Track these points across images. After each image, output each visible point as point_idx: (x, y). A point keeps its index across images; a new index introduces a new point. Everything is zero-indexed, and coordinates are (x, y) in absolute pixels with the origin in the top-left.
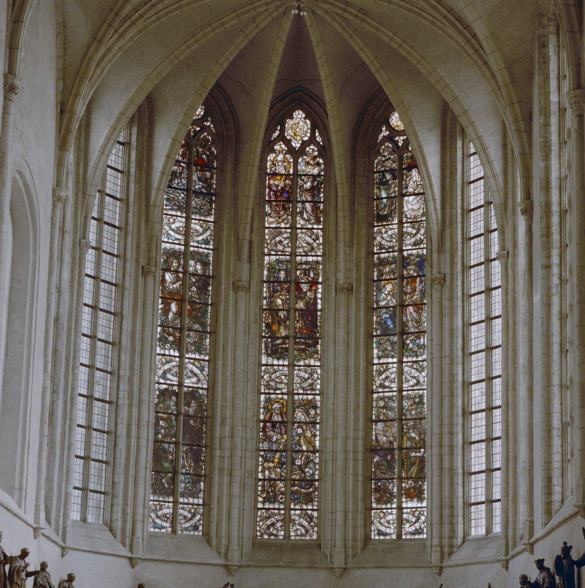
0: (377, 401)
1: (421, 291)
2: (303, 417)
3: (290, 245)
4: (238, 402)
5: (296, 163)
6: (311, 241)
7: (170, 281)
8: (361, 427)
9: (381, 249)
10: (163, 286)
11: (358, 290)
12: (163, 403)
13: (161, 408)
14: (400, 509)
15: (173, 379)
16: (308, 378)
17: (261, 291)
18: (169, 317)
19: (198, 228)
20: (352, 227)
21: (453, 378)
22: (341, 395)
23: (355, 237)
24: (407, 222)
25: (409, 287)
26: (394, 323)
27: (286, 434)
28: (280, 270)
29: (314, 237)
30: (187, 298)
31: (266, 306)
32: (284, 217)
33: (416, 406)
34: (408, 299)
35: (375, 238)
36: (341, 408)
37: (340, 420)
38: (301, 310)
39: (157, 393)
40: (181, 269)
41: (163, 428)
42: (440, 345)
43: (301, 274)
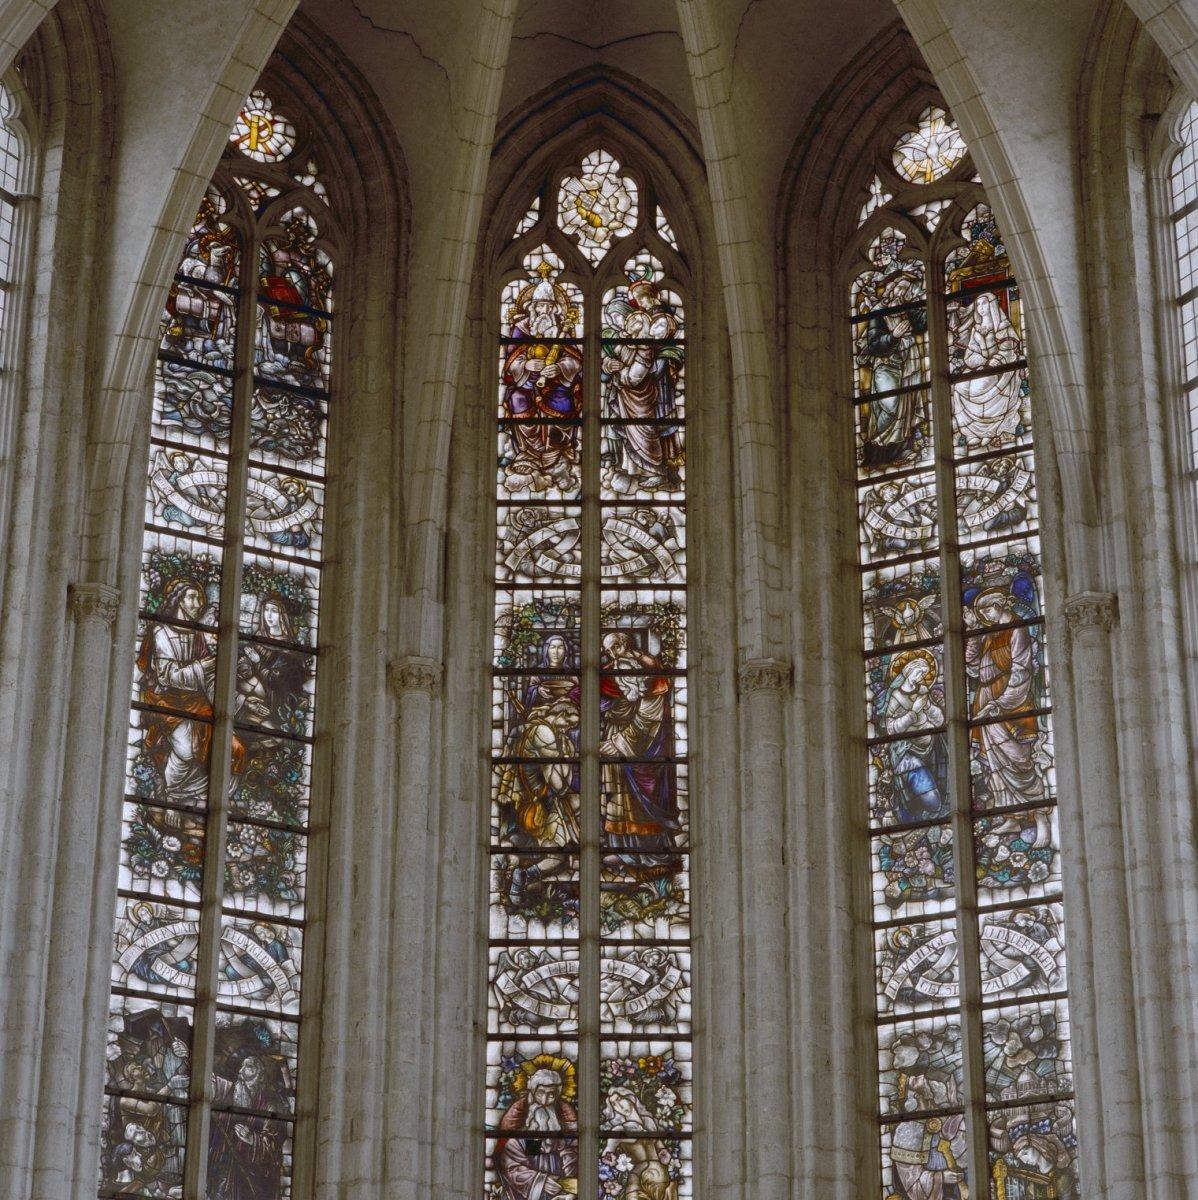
0: (891, 1049)
1: (1029, 670)
2: (634, 1116)
3: (578, 554)
4: (403, 1056)
5: (594, 307)
6: (647, 541)
7: (170, 655)
8: (840, 1136)
9: (883, 550)
10: (147, 669)
11: (813, 681)
12: (138, 1060)
13: (131, 1079)
15: (177, 981)
16: (650, 984)
17: (485, 702)
18: (168, 771)
19: (271, 492)
20: (784, 482)
21: (1167, 936)
22: (766, 1030)
23: (796, 513)
24: (967, 460)
25: (985, 662)
26: (939, 784)
27: (575, 1175)
28: (545, 635)
29: (657, 528)
30: (231, 711)
31: (501, 748)
32: (557, 471)
33: (1031, 1057)
34: (983, 701)
35: (861, 522)
36: (769, 1071)
37: (766, 1112)
38: (621, 759)
39: (120, 1025)
40: (209, 620)
41: (140, 1148)
42: (1112, 825)
43: (616, 645)
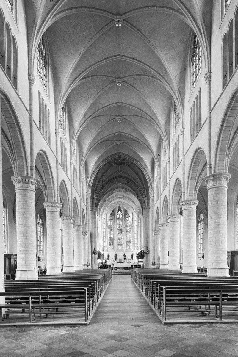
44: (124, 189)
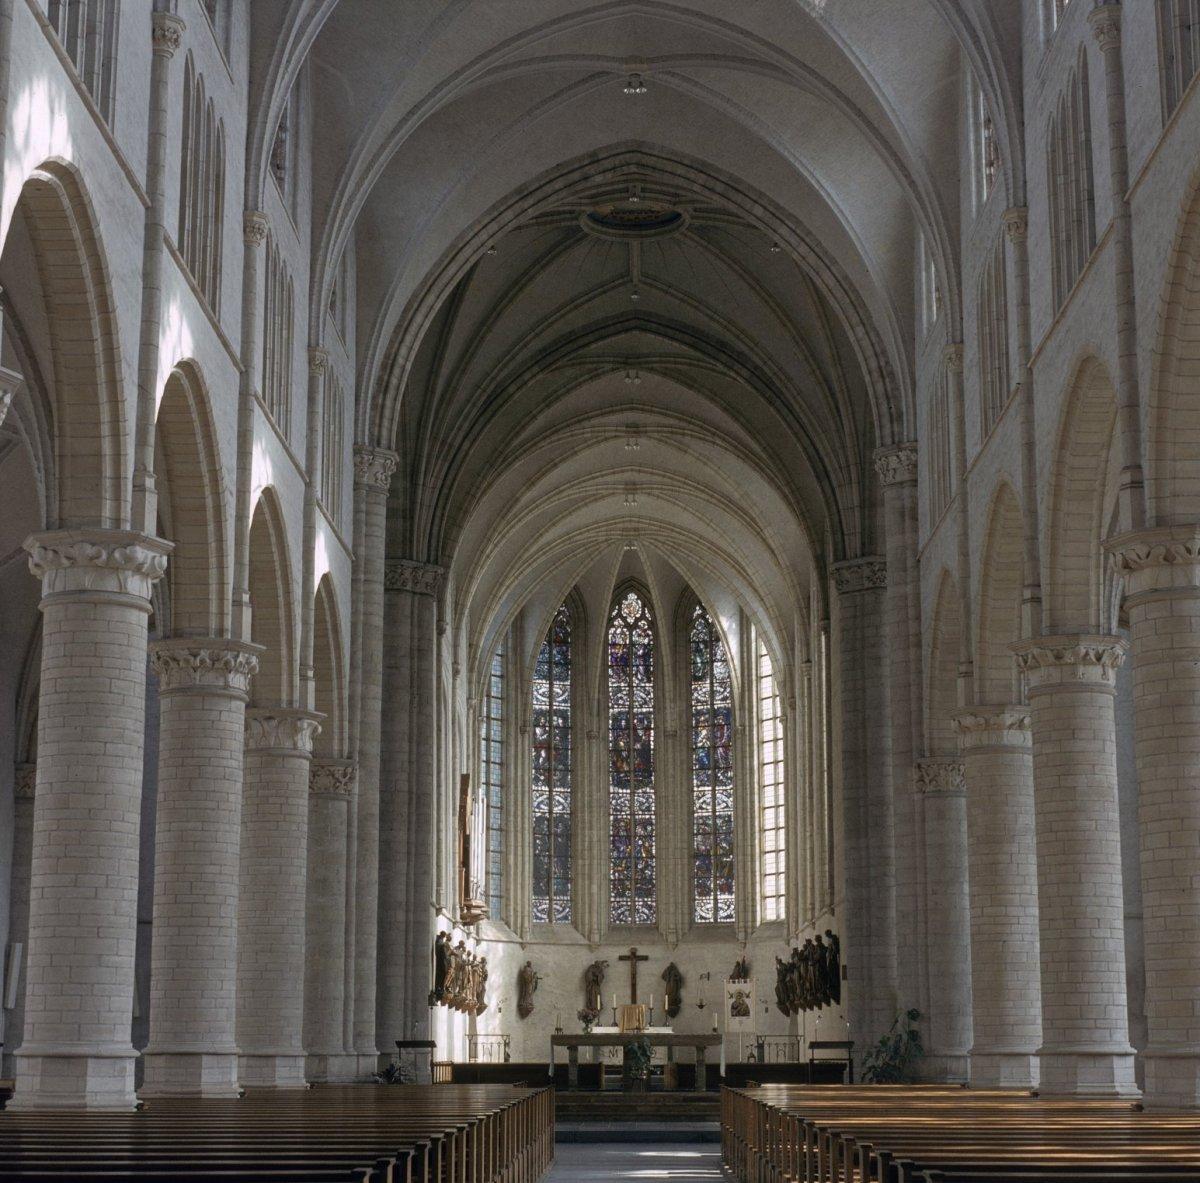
5: (631, 635)
6: (644, 696)
14: (716, 900)
44: (672, 421)
